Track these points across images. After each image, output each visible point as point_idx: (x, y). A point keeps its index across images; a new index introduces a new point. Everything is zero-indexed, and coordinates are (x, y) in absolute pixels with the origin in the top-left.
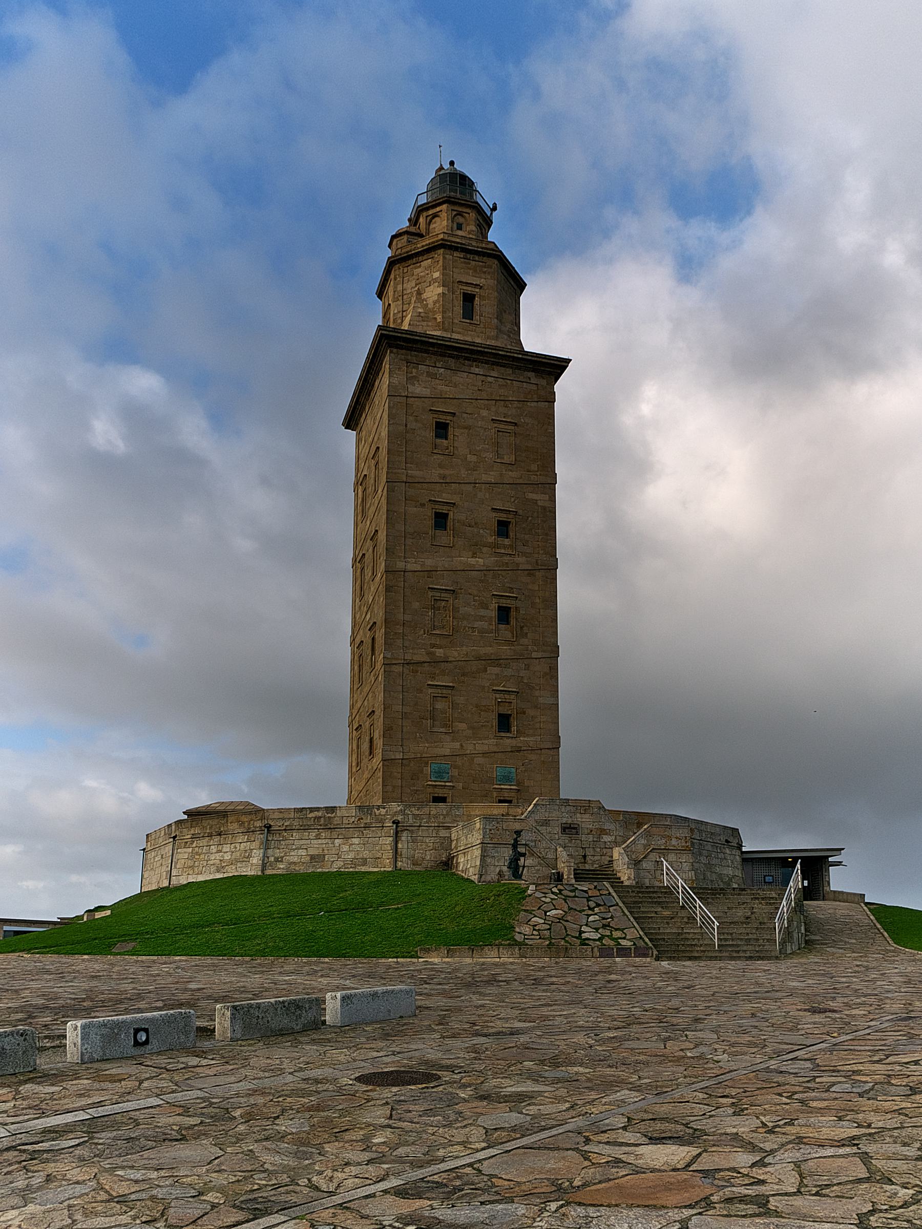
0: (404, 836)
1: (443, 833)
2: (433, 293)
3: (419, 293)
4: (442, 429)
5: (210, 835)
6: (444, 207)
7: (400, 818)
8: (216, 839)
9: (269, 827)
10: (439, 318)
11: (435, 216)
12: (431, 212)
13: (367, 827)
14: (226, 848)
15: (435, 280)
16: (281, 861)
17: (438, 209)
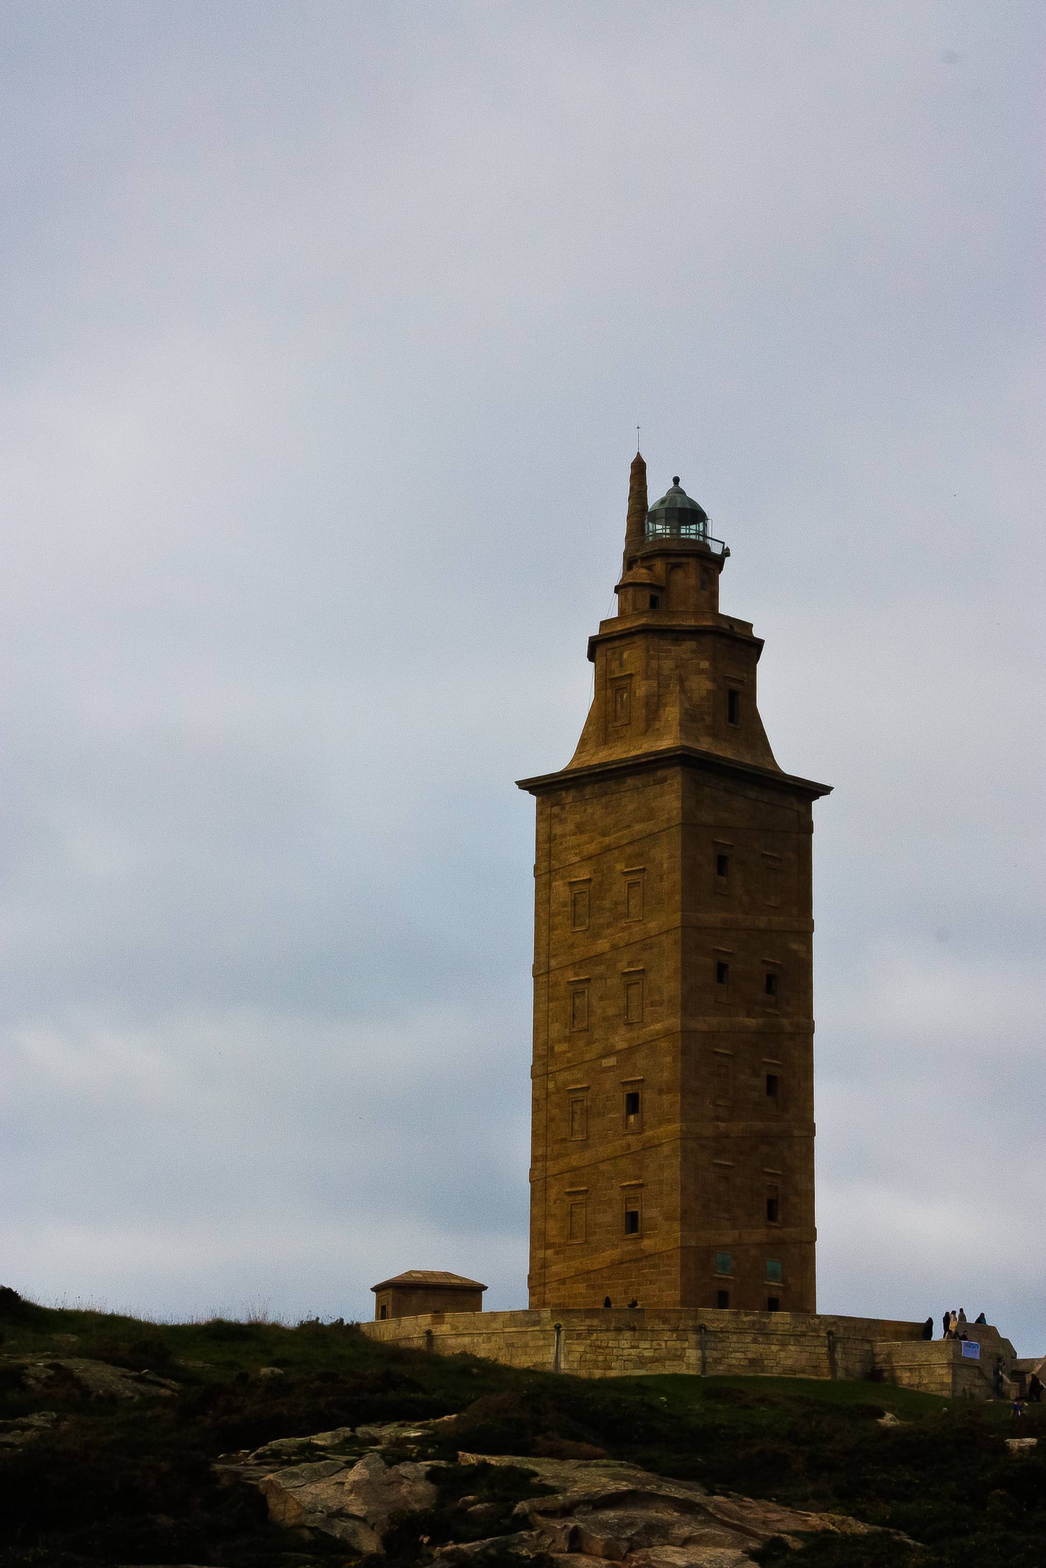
0: (839, 1347)
1: (867, 1347)
2: (701, 685)
3: (681, 681)
4: (722, 864)
5: (619, 1330)
6: (692, 561)
7: (833, 1329)
8: (628, 1334)
9: (701, 1329)
10: (708, 720)
11: (677, 566)
12: (673, 560)
13: (803, 1334)
14: (644, 1345)
15: (702, 672)
16: (720, 1363)
17: (684, 560)
